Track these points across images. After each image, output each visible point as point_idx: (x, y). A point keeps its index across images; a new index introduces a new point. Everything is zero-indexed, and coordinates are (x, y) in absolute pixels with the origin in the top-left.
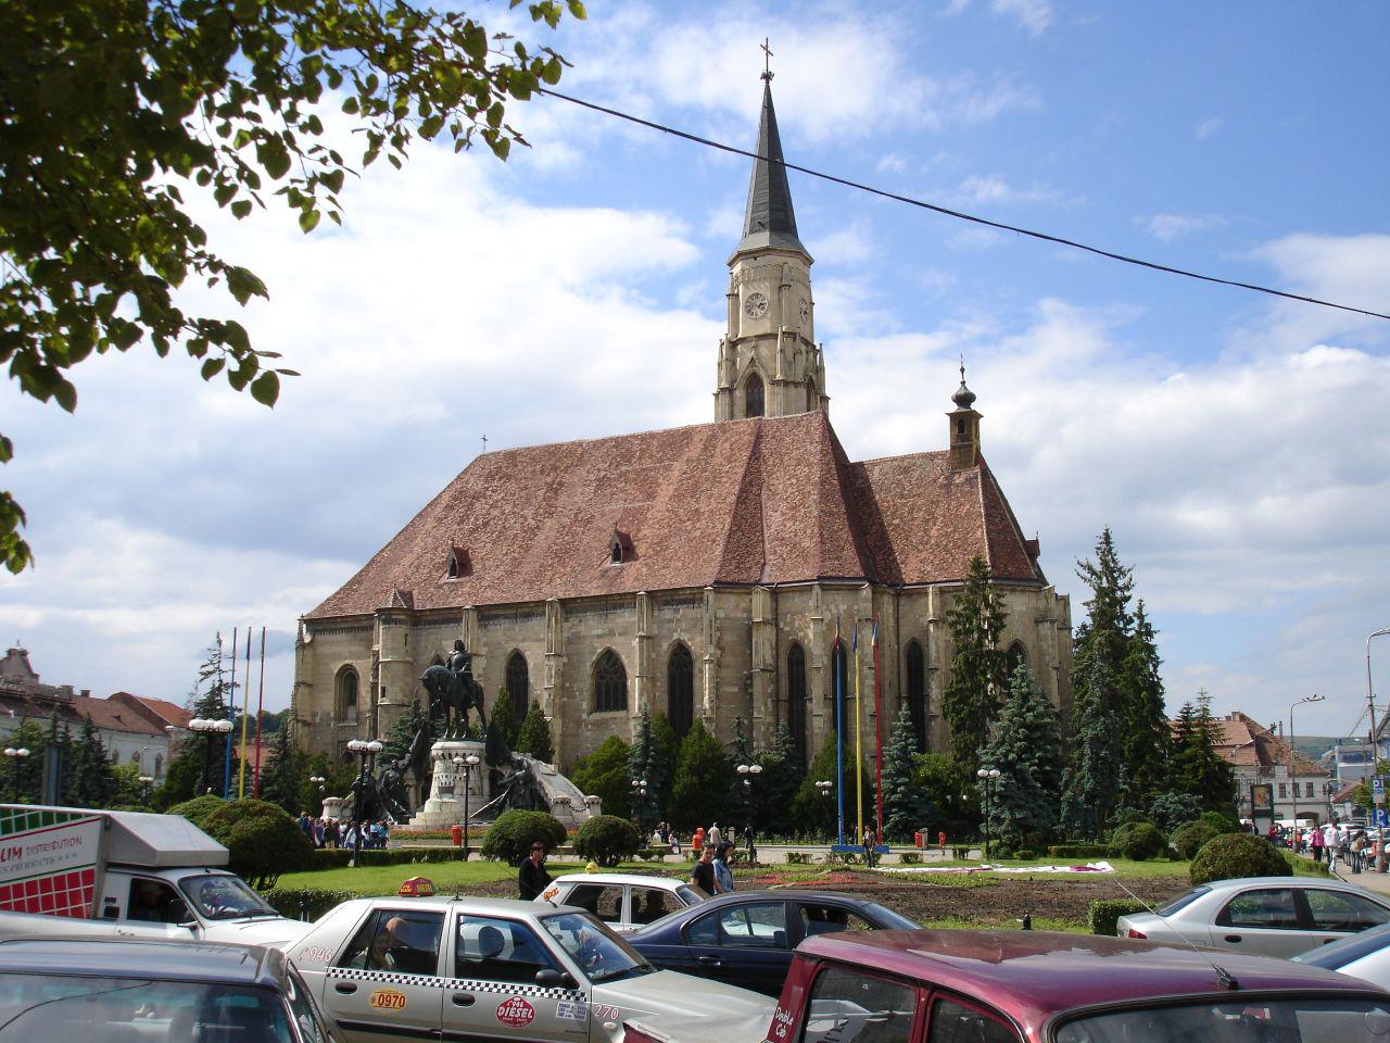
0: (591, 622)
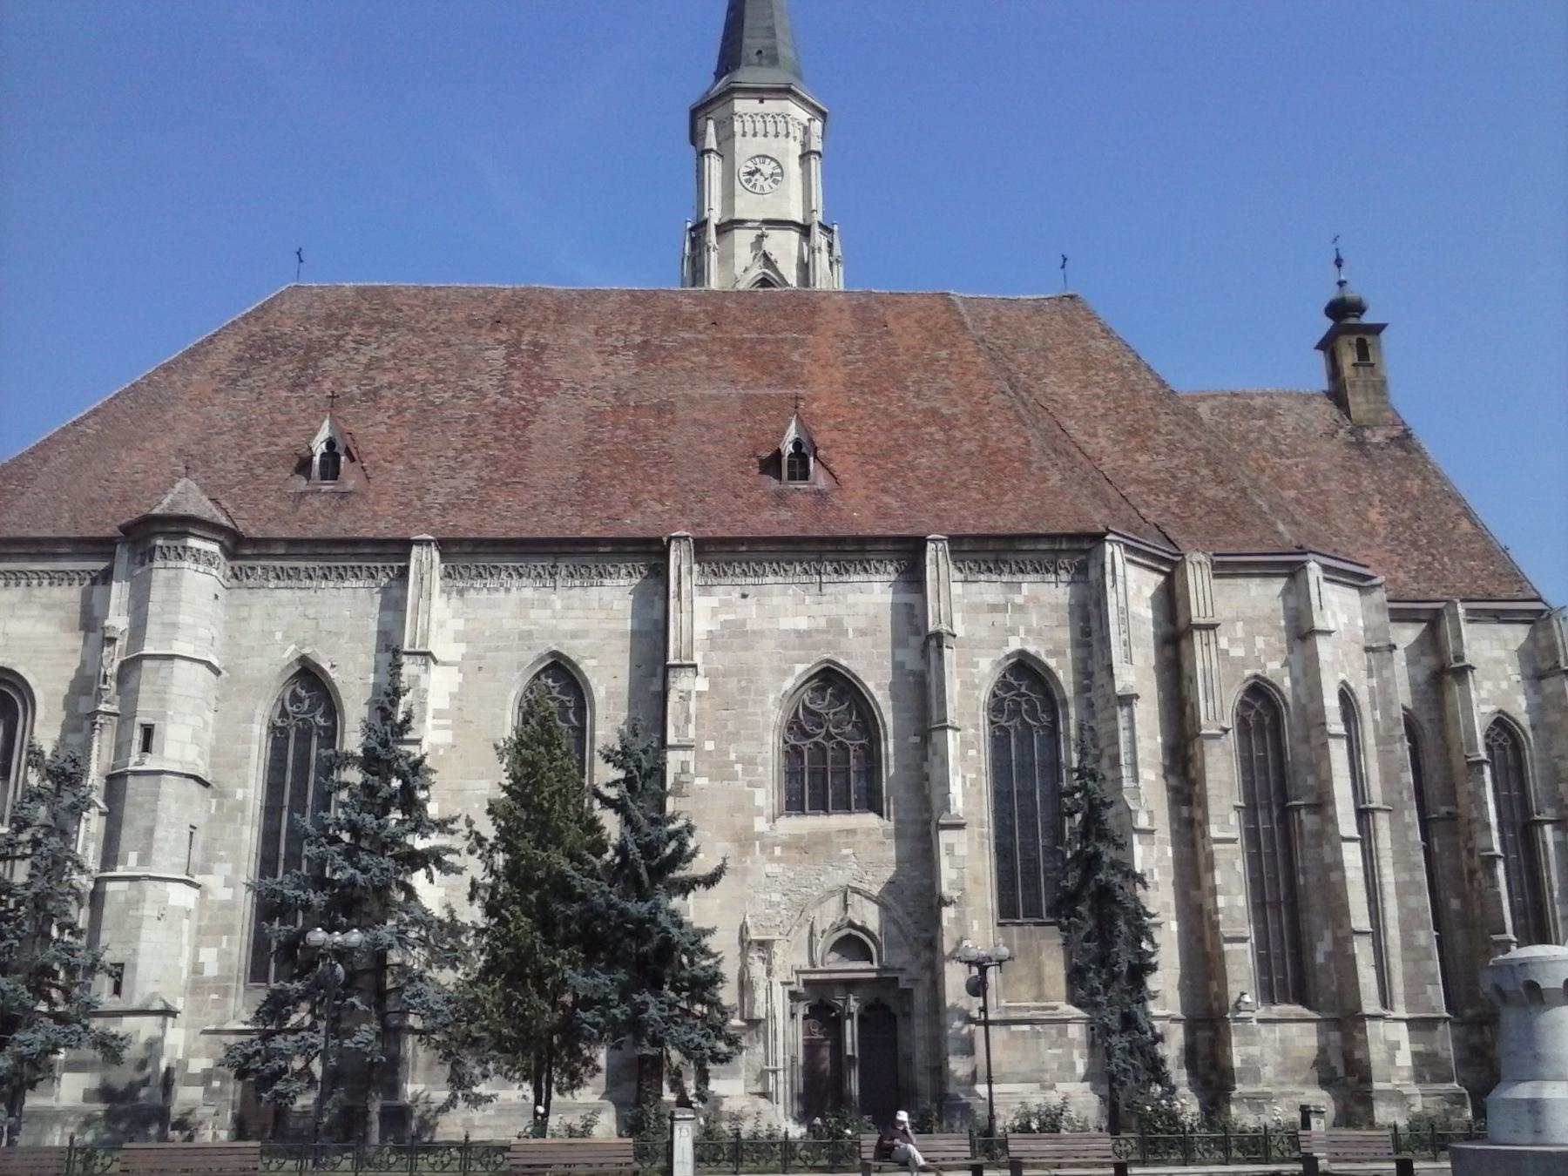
0: (776, 600)
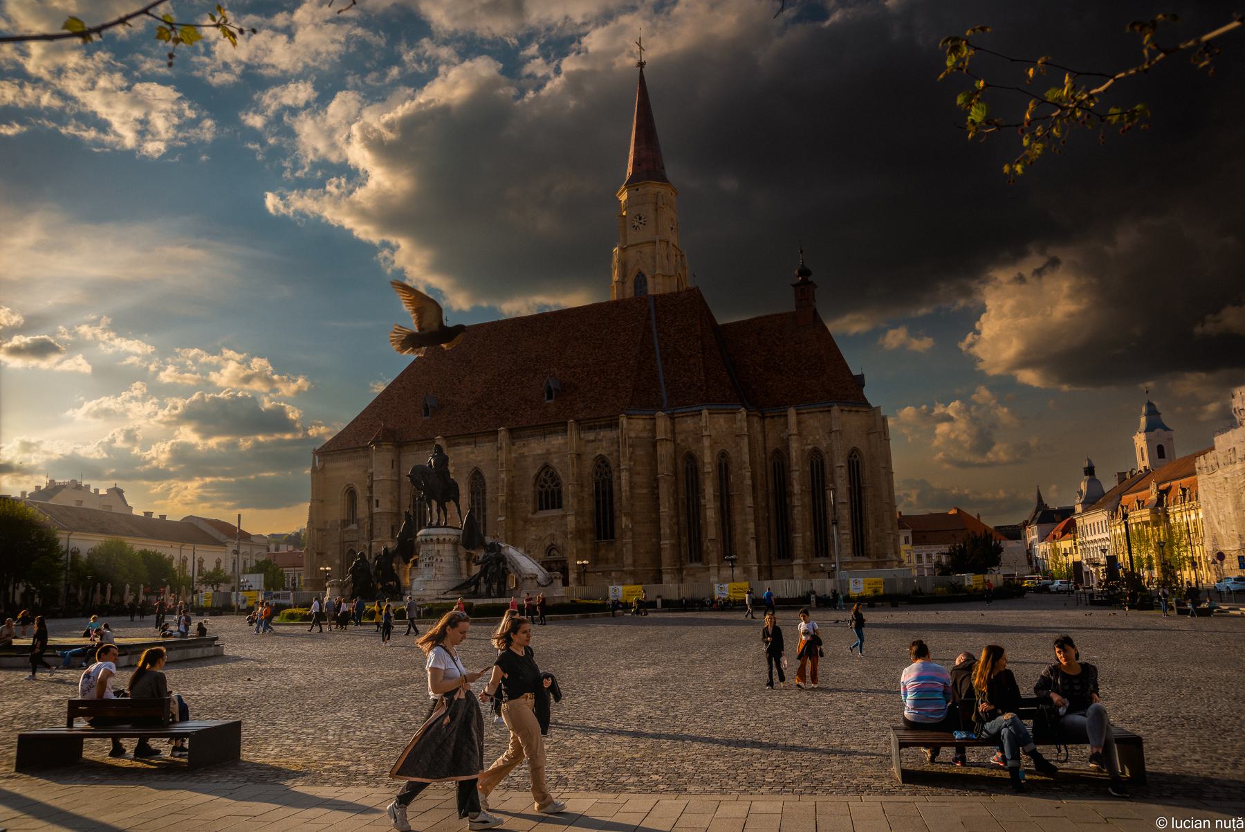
0: (532, 445)
